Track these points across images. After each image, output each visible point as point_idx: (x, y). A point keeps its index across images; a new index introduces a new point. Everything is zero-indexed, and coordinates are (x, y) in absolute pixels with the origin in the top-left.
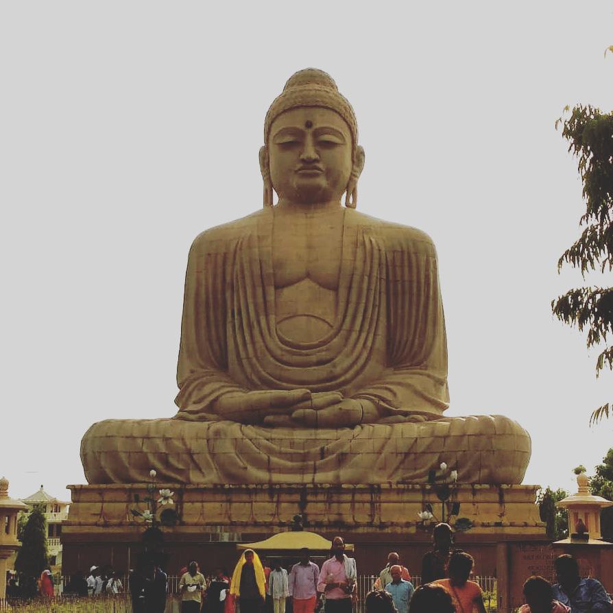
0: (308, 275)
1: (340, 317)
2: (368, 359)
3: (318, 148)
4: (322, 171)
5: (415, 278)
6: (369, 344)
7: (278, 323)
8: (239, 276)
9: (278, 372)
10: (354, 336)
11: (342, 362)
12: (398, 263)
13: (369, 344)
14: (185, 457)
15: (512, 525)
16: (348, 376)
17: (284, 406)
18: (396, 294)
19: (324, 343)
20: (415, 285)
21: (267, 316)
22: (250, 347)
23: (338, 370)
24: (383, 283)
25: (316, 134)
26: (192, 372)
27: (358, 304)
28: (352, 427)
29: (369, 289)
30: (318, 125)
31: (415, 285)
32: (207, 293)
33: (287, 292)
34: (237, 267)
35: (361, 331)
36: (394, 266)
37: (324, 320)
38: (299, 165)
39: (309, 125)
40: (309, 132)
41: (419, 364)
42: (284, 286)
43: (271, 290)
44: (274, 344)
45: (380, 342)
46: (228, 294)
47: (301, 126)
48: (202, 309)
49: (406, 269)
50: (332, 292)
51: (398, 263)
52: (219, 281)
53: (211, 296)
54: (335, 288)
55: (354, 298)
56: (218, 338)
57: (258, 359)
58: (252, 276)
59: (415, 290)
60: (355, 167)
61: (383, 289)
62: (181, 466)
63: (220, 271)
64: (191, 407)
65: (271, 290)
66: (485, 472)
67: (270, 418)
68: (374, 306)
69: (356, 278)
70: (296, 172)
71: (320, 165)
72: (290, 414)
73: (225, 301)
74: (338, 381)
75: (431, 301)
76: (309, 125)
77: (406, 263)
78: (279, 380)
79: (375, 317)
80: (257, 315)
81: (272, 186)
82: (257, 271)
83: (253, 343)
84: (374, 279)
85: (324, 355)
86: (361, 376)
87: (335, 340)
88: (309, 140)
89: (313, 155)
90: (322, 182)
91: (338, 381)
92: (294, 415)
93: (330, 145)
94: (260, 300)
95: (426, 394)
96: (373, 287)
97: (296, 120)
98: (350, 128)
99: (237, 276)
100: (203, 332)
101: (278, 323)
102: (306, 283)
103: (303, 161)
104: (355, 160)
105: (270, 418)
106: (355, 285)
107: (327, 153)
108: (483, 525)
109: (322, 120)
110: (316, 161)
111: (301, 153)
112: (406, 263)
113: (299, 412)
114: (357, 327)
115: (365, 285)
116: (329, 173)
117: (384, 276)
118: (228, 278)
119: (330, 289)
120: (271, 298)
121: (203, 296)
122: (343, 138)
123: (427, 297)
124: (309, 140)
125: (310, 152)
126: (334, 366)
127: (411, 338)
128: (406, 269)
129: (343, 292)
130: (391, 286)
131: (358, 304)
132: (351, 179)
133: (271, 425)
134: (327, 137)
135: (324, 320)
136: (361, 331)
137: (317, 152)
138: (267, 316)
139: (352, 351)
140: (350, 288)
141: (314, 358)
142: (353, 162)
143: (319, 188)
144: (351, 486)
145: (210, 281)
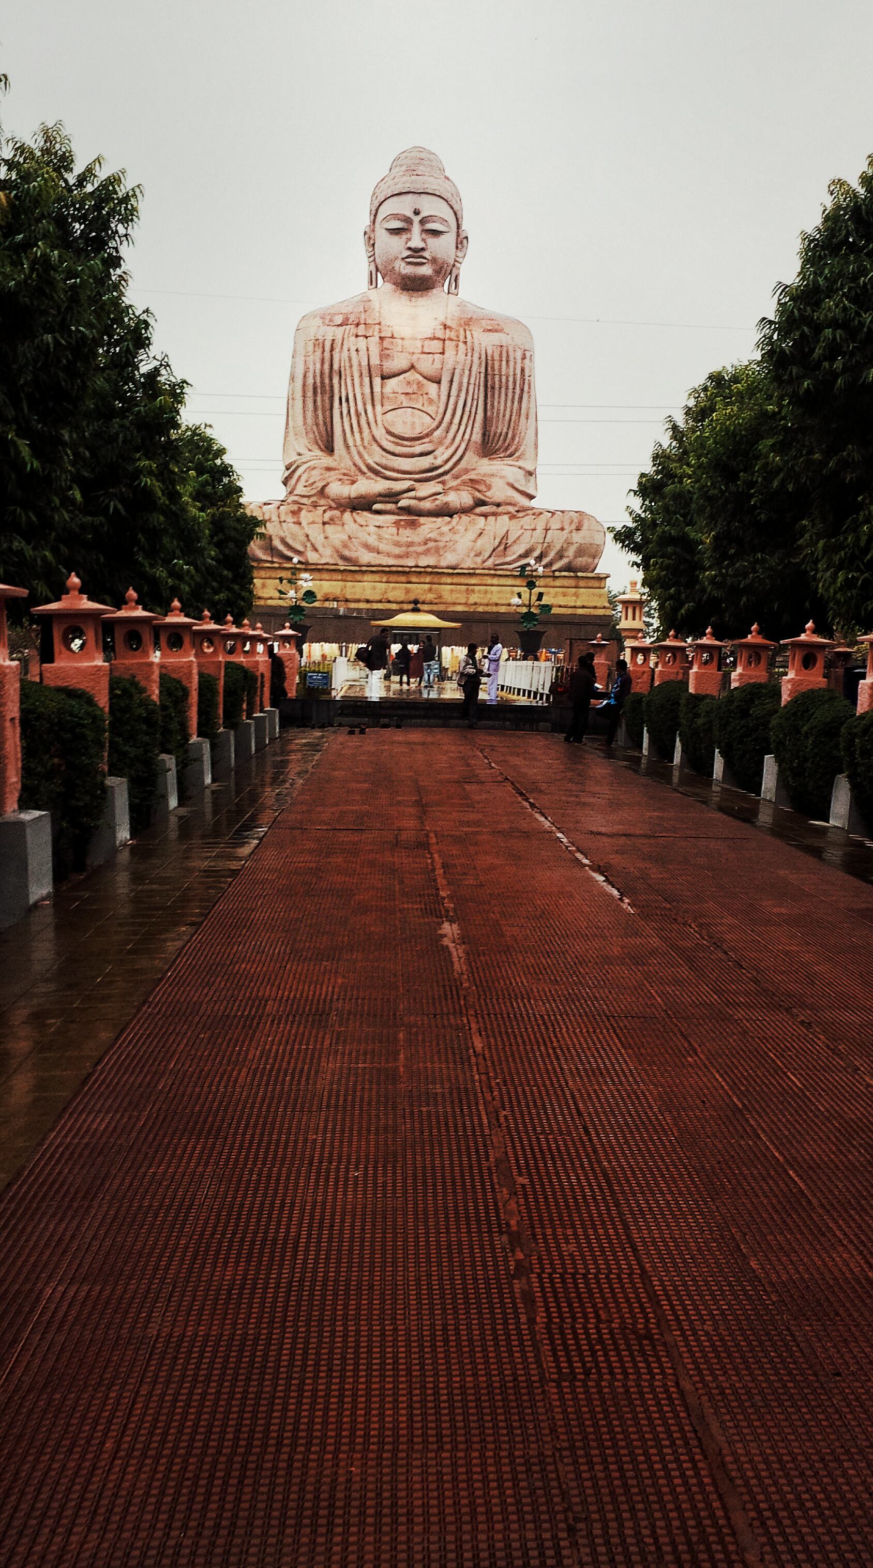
1: (441, 410)
2: (464, 453)
3: (424, 236)
5: (511, 373)
6: (467, 437)
8: (347, 364)
9: (384, 462)
10: (454, 427)
11: (442, 454)
12: (497, 357)
13: (467, 437)
14: (304, 539)
15: (583, 607)
16: (447, 467)
17: (392, 496)
18: (493, 388)
19: (427, 435)
20: (511, 379)
21: (373, 405)
22: (357, 435)
23: (439, 462)
24: (483, 375)
25: (422, 222)
26: (299, 454)
27: (458, 396)
28: (451, 516)
29: (469, 383)
30: (424, 214)
31: (511, 379)
32: (314, 377)
33: (392, 383)
34: (345, 354)
35: (460, 424)
36: (493, 360)
38: (409, 253)
39: (417, 213)
40: (416, 219)
41: (510, 456)
42: (389, 377)
43: (377, 381)
44: (380, 433)
45: (477, 436)
46: (336, 381)
47: (409, 214)
48: (310, 394)
49: (504, 363)
50: (435, 385)
51: (497, 357)
52: (327, 366)
53: (318, 381)
54: (439, 382)
55: (454, 392)
56: (325, 423)
57: (365, 447)
58: (360, 365)
59: (511, 387)
60: (460, 254)
61: (482, 384)
62: (301, 548)
63: (327, 355)
64: (300, 490)
65: (377, 381)
66: (565, 561)
67: (376, 507)
69: (457, 371)
71: (426, 254)
72: (397, 503)
73: (332, 387)
74: (440, 471)
75: (525, 396)
76: (417, 213)
77: (504, 359)
78: (386, 468)
80: (365, 404)
81: (377, 270)
82: (364, 363)
83: (361, 432)
84: (473, 373)
85: (427, 447)
86: (459, 467)
87: (437, 434)
88: (416, 228)
89: (421, 245)
90: (426, 270)
91: (440, 471)
92: (400, 504)
93: (436, 233)
94: (367, 390)
95: (517, 485)
96: (472, 381)
97: (404, 206)
98: (455, 214)
100: (310, 414)
103: (409, 249)
105: (376, 507)
106: (456, 379)
107: (432, 242)
108: (560, 606)
109: (429, 206)
110: (423, 249)
111: (409, 239)
112: (504, 359)
113: (403, 503)
114: (456, 420)
115: (465, 380)
116: (434, 261)
117: (483, 370)
118: (336, 367)
120: (377, 389)
121: (310, 381)
122: (449, 226)
123: (522, 390)
124: (416, 228)
125: (416, 242)
126: (435, 458)
127: (505, 430)
130: (489, 378)
131: (458, 396)
133: (378, 512)
134: (430, 226)
136: (460, 424)
137: (424, 240)
138: (373, 405)
139: (452, 443)
140: (451, 381)
141: (418, 449)
144: (451, 571)
145: (318, 366)
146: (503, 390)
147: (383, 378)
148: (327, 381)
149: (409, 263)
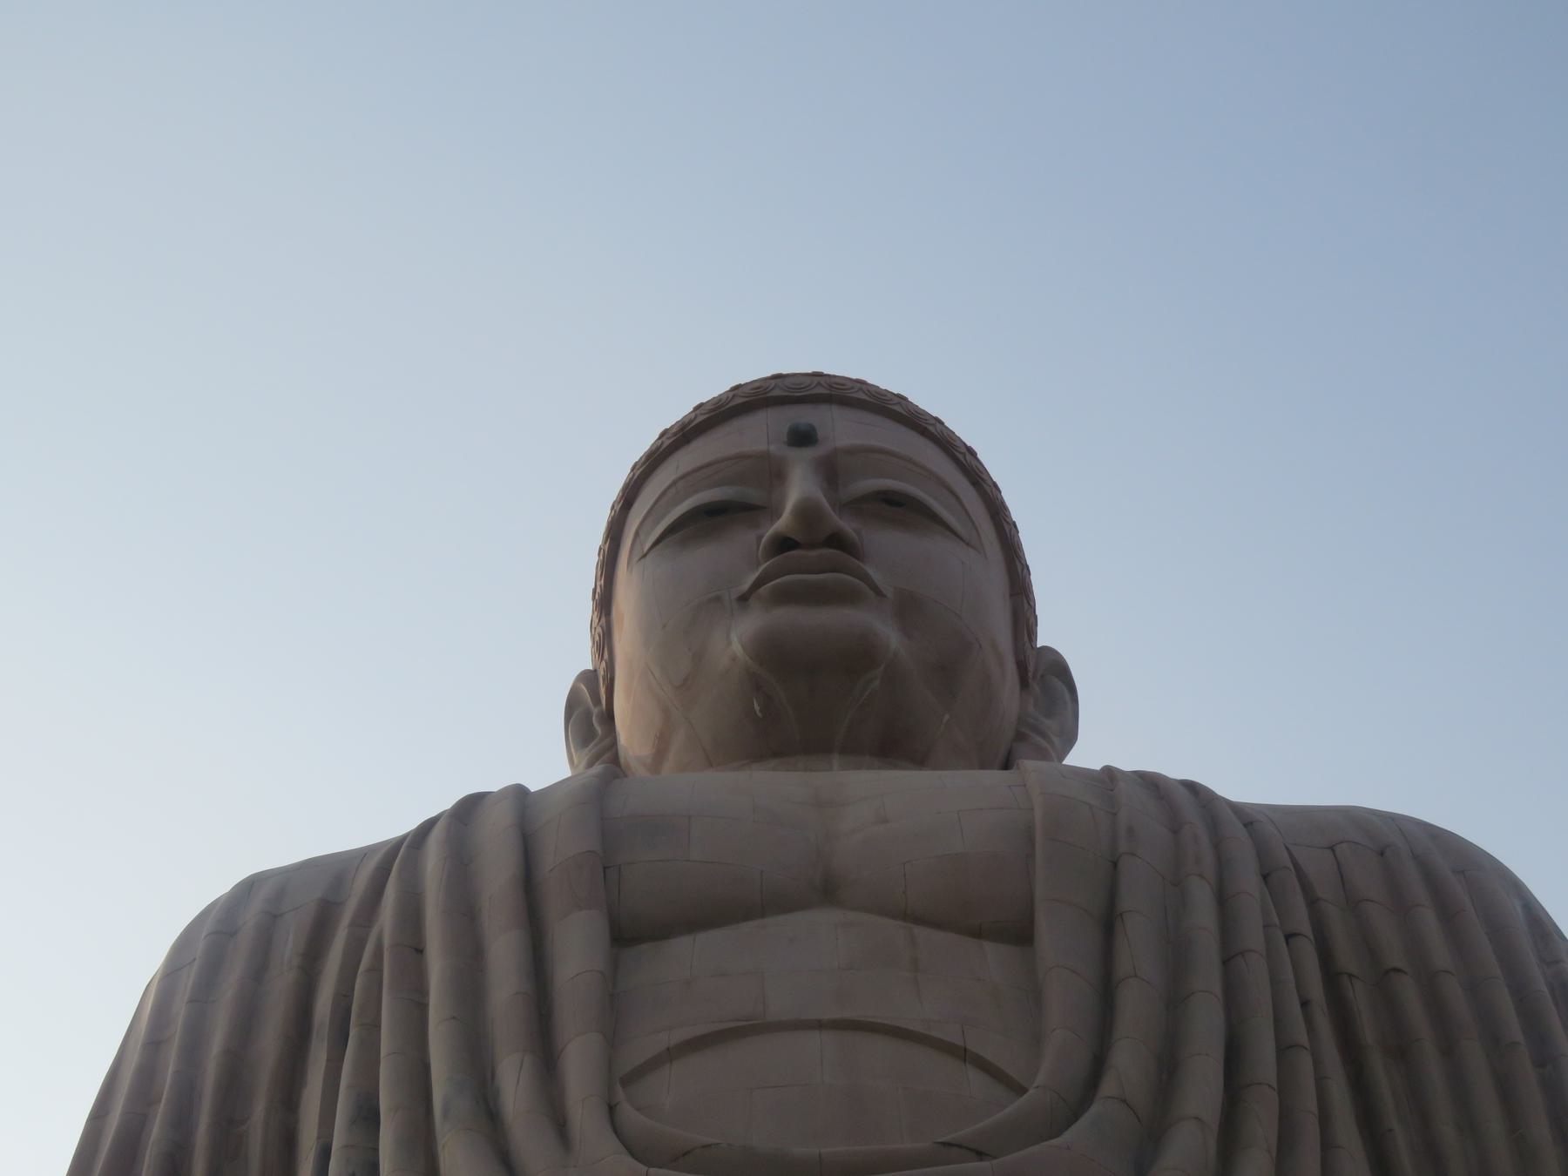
0: (827, 890)
4: (879, 592)
7: (628, 1080)
18: (1401, 1051)
25: (831, 471)
27: (1175, 1001)
29: (1229, 958)
37: (962, 1054)
49: (1428, 918)
59: (1514, 1028)
63: (282, 982)
68: (1284, 1049)
70: (744, 599)
73: (288, 1141)
79: (1310, 1102)
99: (376, 969)
101: (620, 1081)
102: (822, 920)
103: (783, 544)
104: (1036, 688)
116: (909, 608)
119: (978, 933)
128: (1428, 918)
129: (1061, 941)
130: (1360, 998)
131: (1175, 1001)
132: (1020, 737)
135: (962, 1054)
142: (1024, 683)
143: (859, 657)
146: (1474, 1054)
147: (627, 934)
148: (259, 1109)
149: (786, 597)
